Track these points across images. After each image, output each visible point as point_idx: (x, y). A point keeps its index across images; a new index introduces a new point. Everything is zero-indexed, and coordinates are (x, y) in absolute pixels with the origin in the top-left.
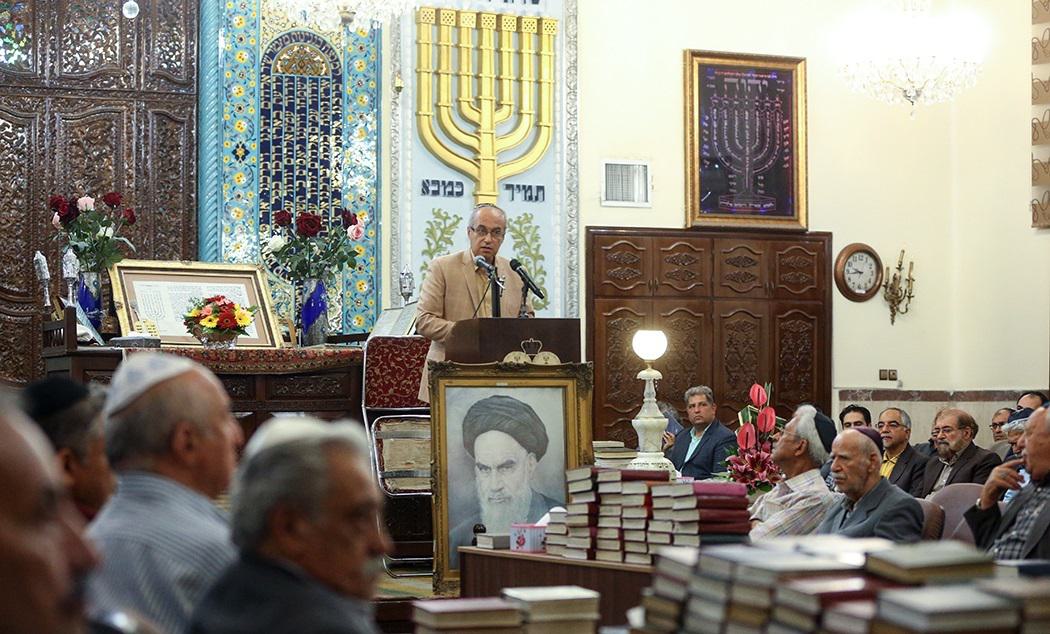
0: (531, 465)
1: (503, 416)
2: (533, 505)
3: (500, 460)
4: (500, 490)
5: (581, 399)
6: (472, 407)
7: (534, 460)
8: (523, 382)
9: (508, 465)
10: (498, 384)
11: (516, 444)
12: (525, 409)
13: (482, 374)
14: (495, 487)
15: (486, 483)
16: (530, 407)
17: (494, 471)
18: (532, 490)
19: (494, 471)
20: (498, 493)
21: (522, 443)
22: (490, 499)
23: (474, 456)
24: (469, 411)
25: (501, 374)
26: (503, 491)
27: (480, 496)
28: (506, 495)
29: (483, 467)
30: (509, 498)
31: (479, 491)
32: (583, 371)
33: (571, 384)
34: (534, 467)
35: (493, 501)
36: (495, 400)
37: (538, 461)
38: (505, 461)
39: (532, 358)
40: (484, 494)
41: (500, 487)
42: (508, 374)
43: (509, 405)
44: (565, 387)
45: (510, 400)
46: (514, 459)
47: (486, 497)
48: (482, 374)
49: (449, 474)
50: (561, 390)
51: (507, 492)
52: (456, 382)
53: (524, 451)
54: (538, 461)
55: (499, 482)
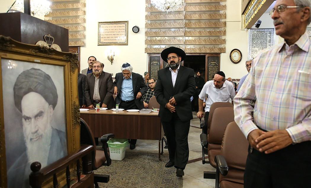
0: (51, 112)
1: (37, 82)
2: (52, 137)
3: (36, 112)
4: (36, 132)
5: (72, 73)
6: (20, 75)
7: (52, 109)
8: (45, 60)
9: (40, 115)
10: (35, 61)
11: (43, 100)
12: (47, 78)
13: (28, 52)
14: (34, 130)
15: (29, 128)
16: (49, 77)
17: (33, 120)
18: (52, 128)
19: (33, 120)
20: (36, 134)
21: (46, 98)
22: (31, 139)
23: (21, 111)
24: (18, 78)
25: (39, 54)
26: (38, 132)
27: (26, 139)
28: (40, 135)
29: (27, 118)
30: (41, 136)
31: (25, 135)
32: (74, 58)
33: (68, 65)
34: (52, 114)
35: (33, 140)
36: (33, 71)
37: (54, 109)
38: (38, 112)
39: (50, 46)
40: (27, 138)
41: (36, 130)
42: (42, 55)
43: (40, 75)
44: (64, 66)
45: (40, 72)
46: (43, 110)
47: (29, 138)
48: (28, 52)
49: (6, 127)
50: (63, 67)
51: (40, 132)
52: (9, 55)
53: (47, 105)
54: (54, 109)
55: (35, 127)
